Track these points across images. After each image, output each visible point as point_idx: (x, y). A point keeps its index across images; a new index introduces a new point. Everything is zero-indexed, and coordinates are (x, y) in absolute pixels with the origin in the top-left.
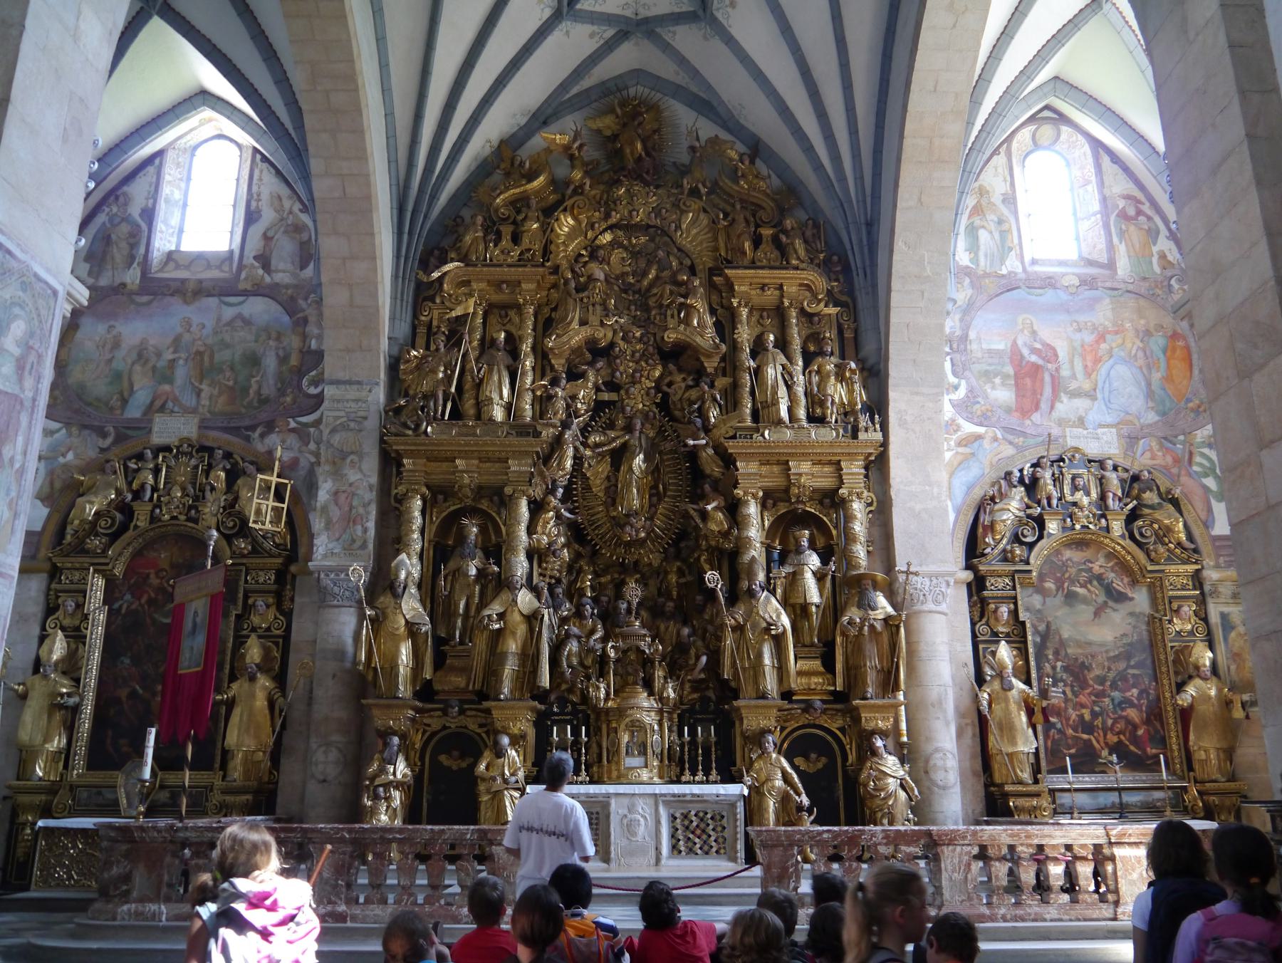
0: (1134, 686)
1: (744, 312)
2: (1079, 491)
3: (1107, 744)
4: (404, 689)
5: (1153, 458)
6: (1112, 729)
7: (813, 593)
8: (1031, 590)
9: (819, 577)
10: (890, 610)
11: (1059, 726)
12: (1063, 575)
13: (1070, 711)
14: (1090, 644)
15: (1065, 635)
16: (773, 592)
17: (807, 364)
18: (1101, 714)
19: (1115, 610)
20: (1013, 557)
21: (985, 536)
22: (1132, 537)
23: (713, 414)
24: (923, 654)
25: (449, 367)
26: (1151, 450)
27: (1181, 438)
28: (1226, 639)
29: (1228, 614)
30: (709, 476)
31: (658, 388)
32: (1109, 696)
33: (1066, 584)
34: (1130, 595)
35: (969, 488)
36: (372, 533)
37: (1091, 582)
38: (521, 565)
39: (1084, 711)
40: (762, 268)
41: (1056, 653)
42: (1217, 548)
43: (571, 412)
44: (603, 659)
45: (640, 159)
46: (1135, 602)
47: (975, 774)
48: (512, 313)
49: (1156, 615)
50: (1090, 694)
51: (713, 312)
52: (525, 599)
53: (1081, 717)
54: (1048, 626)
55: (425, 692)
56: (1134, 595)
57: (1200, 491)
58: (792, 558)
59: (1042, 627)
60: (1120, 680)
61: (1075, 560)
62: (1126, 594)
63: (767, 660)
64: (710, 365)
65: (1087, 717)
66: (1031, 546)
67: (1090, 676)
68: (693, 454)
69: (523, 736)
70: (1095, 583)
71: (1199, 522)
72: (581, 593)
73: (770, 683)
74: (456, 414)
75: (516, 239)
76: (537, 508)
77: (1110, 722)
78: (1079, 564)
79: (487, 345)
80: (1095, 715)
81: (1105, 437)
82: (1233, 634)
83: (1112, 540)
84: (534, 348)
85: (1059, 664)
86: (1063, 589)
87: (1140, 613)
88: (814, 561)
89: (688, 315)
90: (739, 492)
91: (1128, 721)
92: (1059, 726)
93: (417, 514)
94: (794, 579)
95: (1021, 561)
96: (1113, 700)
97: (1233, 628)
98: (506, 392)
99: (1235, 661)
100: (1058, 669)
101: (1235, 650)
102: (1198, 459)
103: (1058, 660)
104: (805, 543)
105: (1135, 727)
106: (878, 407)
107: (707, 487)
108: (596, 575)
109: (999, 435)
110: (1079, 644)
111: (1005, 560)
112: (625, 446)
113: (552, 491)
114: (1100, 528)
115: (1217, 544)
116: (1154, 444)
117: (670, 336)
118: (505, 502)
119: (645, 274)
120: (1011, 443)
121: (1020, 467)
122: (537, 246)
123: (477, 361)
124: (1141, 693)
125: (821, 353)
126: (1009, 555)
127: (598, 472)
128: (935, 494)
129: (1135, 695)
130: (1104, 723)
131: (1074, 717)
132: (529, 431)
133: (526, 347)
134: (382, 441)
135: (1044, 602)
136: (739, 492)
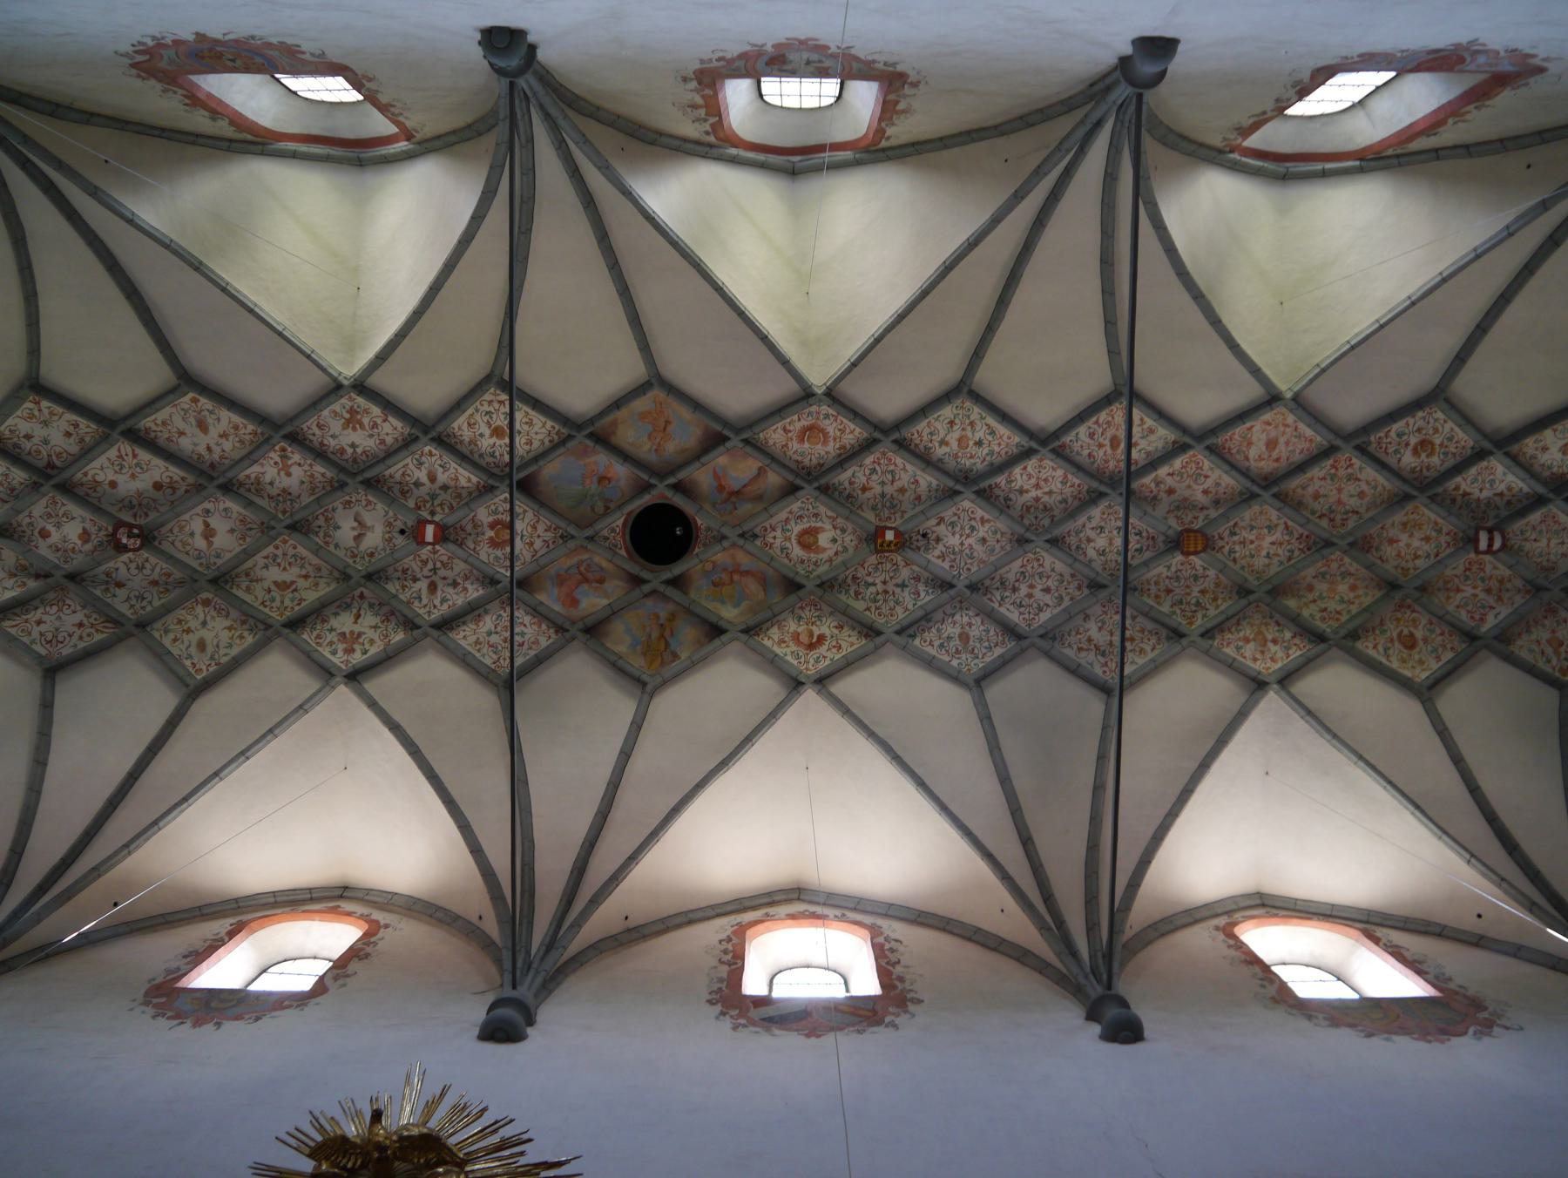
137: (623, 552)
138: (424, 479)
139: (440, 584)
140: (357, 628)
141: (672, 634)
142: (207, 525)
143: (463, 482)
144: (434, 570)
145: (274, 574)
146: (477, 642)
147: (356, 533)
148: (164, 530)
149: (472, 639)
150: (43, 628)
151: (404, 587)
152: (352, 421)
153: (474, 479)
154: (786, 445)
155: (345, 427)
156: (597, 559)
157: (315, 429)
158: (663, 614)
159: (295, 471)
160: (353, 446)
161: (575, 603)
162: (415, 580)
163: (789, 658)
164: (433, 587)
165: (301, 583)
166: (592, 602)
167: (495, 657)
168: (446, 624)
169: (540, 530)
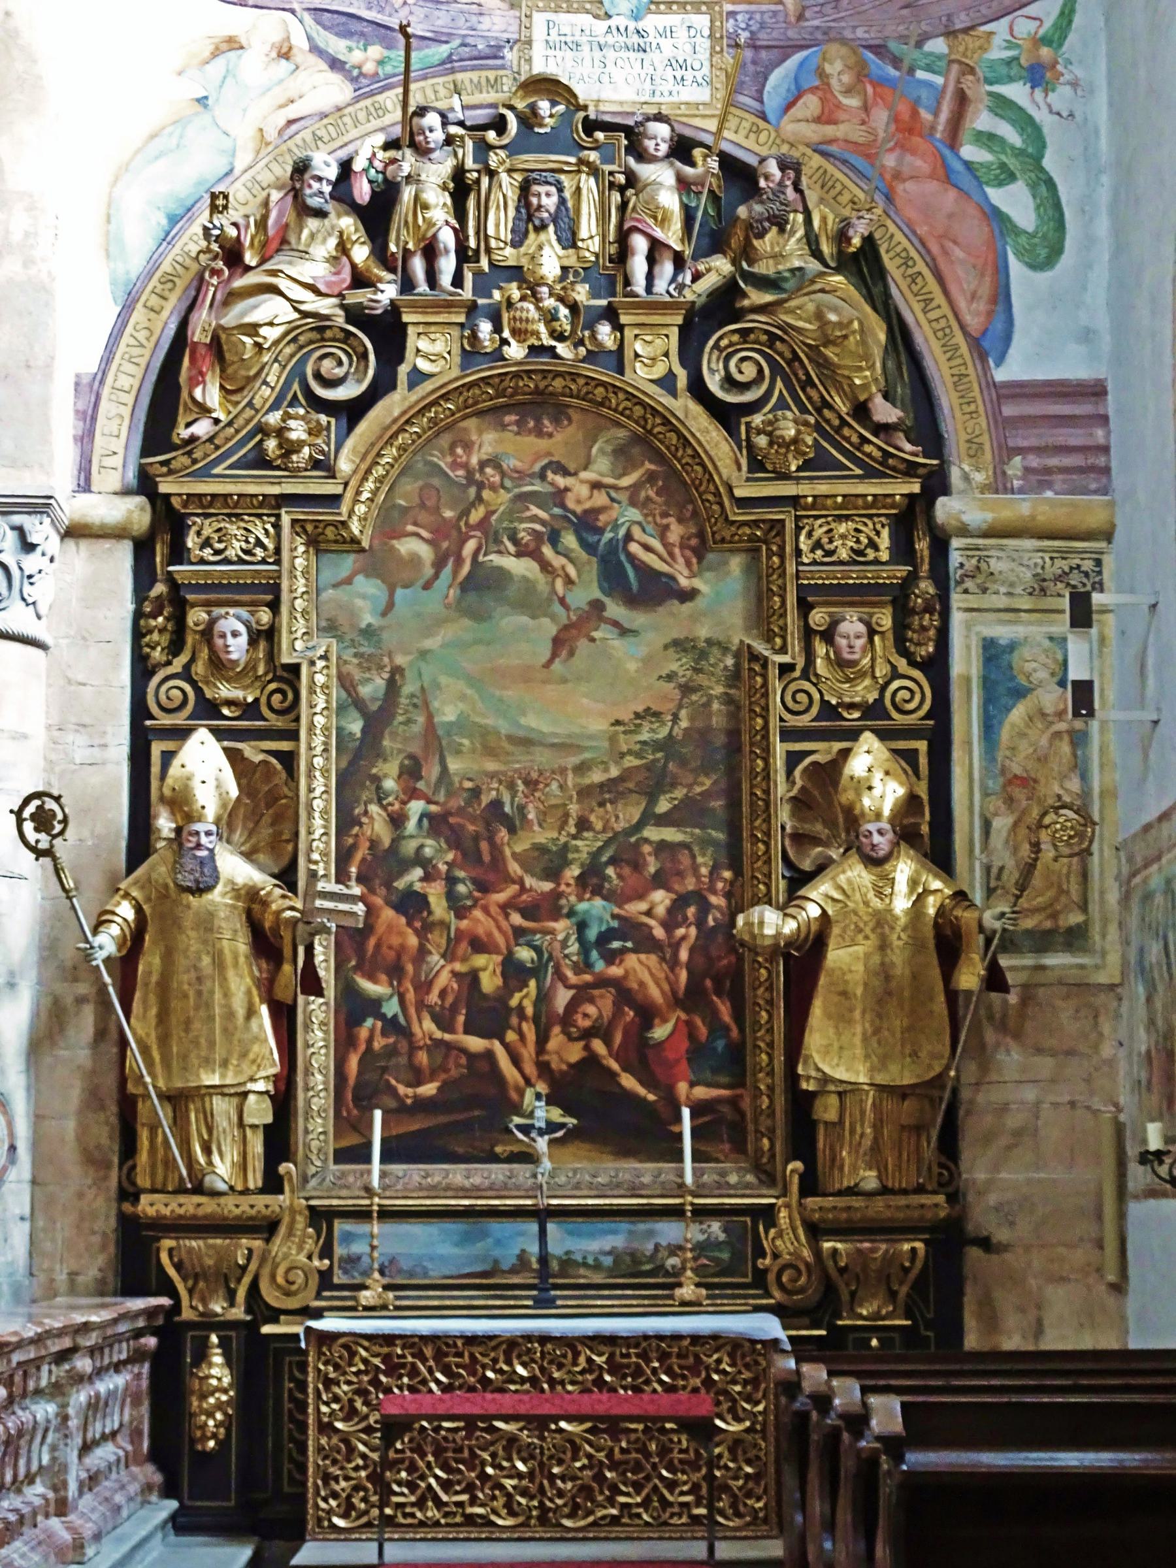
0: (660, 881)
2: (542, 228)
3: (544, 1069)
5: (825, 118)
6: (566, 1021)
8: (348, 563)
11: (391, 1008)
12: (466, 513)
13: (435, 959)
14: (526, 742)
15: (448, 713)
18: (536, 971)
19: (624, 631)
20: (290, 448)
21: (198, 378)
22: (698, 390)
26: (823, 88)
27: (938, 45)
28: (989, 728)
29: (1012, 647)
32: (571, 913)
33: (471, 546)
34: (684, 582)
35: (174, 220)
37: (554, 539)
39: (480, 960)
41: (411, 772)
42: (1001, 424)
46: (700, 603)
47: (92, 1159)
49: (761, 648)
50: (505, 908)
53: (473, 978)
54: (392, 686)
56: (697, 583)
57: (973, 230)
59: (372, 688)
60: (613, 861)
61: (511, 463)
62: (673, 578)
65: (490, 982)
66: (353, 412)
67: (514, 847)
70: (570, 540)
71: (959, 338)
77: (563, 997)
78: (521, 476)
80: (514, 973)
81: (666, 44)
82: (1018, 714)
83: (630, 396)
85: (416, 807)
86: (459, 561)
87: (709, 642)
91: (624, 993)
92: (391, 1008)
95: (316, 464)
96: (582, 926)
97: (1020, 693)
99: (1010, 801)
100: (411, 826)
101: (1017, 770)
102: (982, 120)
103: (413, 794)
105: (647, 1015)
109: (300, 42)
110: (488, 745)
111: (260, 461)
114: (591, 357)
115: (1008, 410)
116: (837, 70)
120: (335, 64)
121: (343, 154)
124: (680, 903)
126: (271, 444)
128: (16, 237)
129: (661, 910)
130: (544, 998)
131: (444, 979)
135: (390, 605)
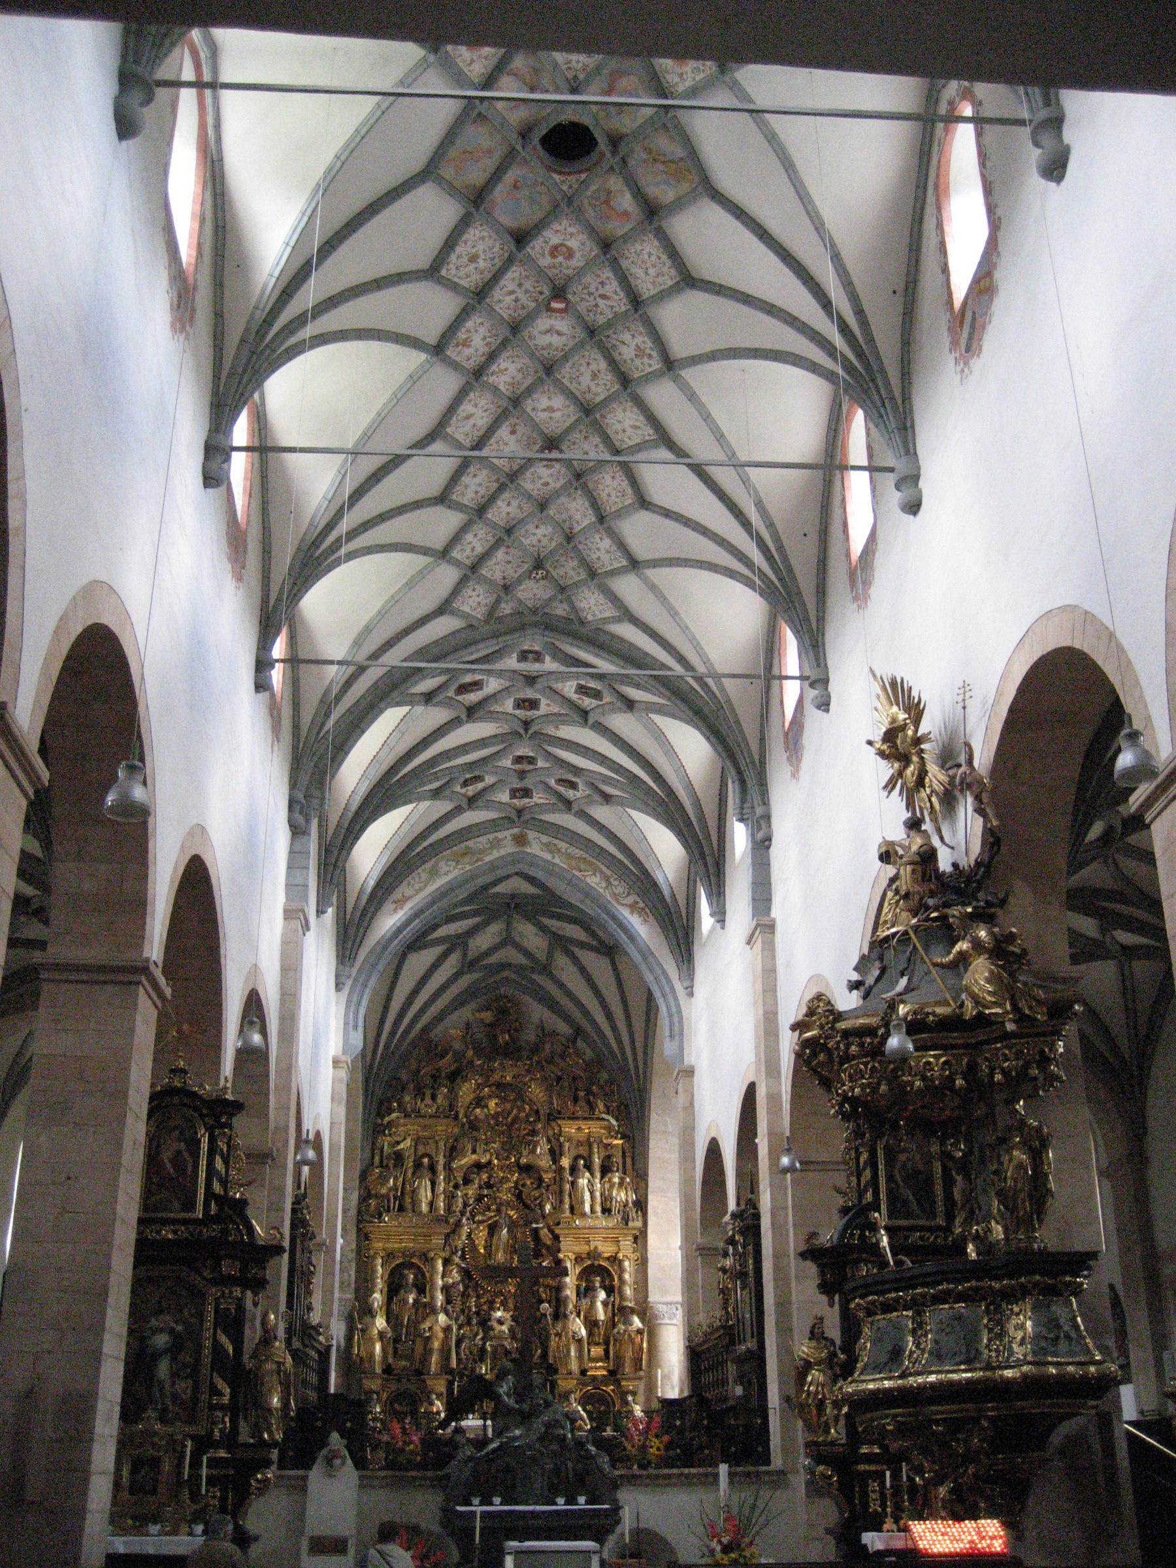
1: (567, 1145)
4: (378, 1370)
7: (601, 1314)
9: (605, 1304)
10: (640, 1325)
16: (578, 1315)
17: (602, 1178)
23: (548, 1207)
24: (661, 1349)
25: (396, 1178)
30: (545, 1244)
31: (516, 1187)
36: (353, 1277)
38: (440, 1298)
40: (577, 1118)
43: (465, 1205)
44: (483, 1350)
45: (507, 1044)
48: (430, 1141)
51: (549, 1141)
52: (442, 1318)
55: (388, 1370)
58: (590, 1293)
63: (573, 1354)
64: (547, 1177)
68: (536, 1232)
69: (442, 1394)
72: (469, 1308)
73: (574, 1366)
74: (401, 1209)
75: (434, 1097)
76: (447, 1262)
79: (418, 1165)
84: (444, 1167)
88: (602, 1295)
89: (535, 1147)
90: (561, 1256)
93: (379, 1268)
94: (592, 1305)
98: (429, 1194)
104: (598, 1285)
106: (641, 1205)
107: (544, 1251)
108: (478, 1297)
112: (496, 1222)
113: (454, 1253)
117: (524, 1161)
118: (430, 1261)
119: (509, 1113)
122: (446, 1104)
123: (413, 1174)
125: (611, 1171)
127: (481, 1236)
132: (440, 1220)
133: (440, 1168)
134: (359, 1222)
136: (561, 1256)
137: (583, 176)
138: (513, 297)
139: (601, 291)
140: (633, 347)
141: (665, 155)
142: (545, 410)
143: (517, 275)
144: (590, 294)
145: (586, 380)
146: (653, 283)
147: (555, 335)
148: (546, 431)
149: (650, 287)
150: (613, 494)
151: (601, 313)
152: (466, 343)
153: (514, 268)
154: (486, 58)
155: (469, 346)
156: (589, 193)
157: (471, 361)
158: (644, 156)
159: (503, 365)
160: (484, 338)
161: (626, 214)
162: (597, 305)
163: (698, 78)
164: (603, 297)
165: (594, 367)
166: (626, 201)
167: (667, 277)
168: (636, 301)
169: (559, 228)
